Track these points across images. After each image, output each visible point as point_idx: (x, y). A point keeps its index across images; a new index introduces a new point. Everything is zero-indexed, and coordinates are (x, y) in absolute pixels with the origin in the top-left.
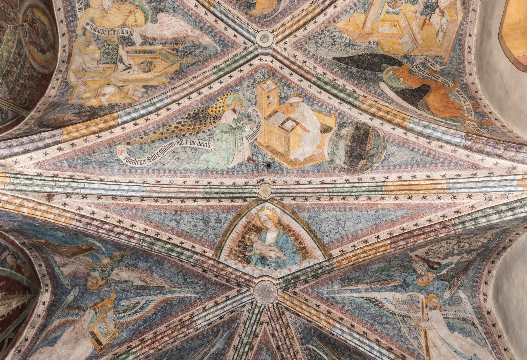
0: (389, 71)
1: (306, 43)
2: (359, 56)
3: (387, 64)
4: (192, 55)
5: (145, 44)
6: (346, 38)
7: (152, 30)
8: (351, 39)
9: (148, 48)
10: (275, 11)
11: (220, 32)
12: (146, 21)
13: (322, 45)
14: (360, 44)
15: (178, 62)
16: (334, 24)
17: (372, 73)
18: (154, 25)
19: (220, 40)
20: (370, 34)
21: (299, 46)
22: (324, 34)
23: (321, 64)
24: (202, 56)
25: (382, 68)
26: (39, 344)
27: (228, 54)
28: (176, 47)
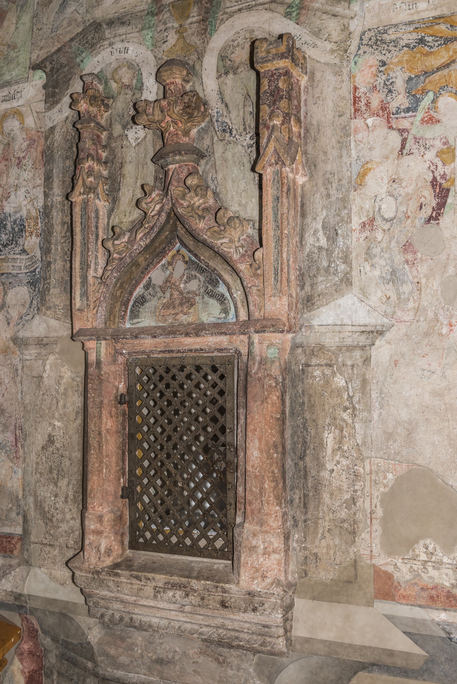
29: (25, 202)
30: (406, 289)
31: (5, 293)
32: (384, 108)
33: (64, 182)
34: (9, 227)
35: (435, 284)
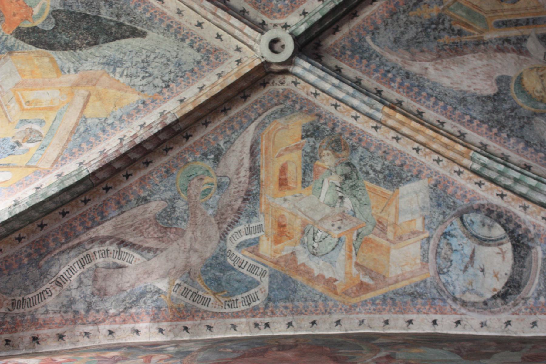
0: (40, 15)
1: (199, 62)
2: (96, 44)
3: (44, 32)
4: (423, 25)
5: (518, 39)
6: (121, 76)
7: (507, 65)
8: (111, 75)
9: (513, 33)
10: (262, 125)
11: (369, 74)
12: (520, 80)
13: (168, 60)
14: (95, 68)
15: (448, 7)
16: (145, 99)
17: (71, 6)
18: (504, 73)
19: (369, 58)
20: (77, 85)
21: (211, 56)
22: (164, 81)
23: (168, 22)
24: (401, 23)
25: (53, 20)
27: (350, 33)
28: (456, 39)
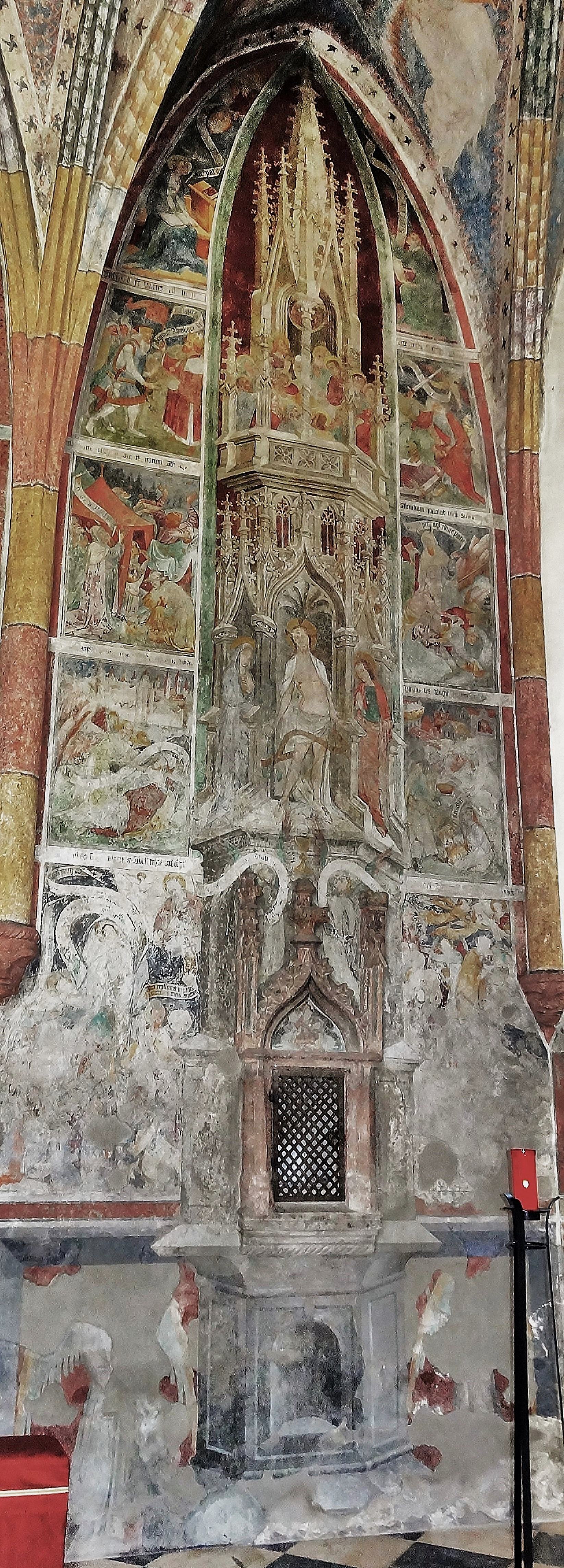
26: (414, 102)
29: (185, 946)
30: (430, 1042)
31: (167, 1013)
32: (417, 939)
33: (219, 938)
34: (169, 962)
35: (443, 1040)
